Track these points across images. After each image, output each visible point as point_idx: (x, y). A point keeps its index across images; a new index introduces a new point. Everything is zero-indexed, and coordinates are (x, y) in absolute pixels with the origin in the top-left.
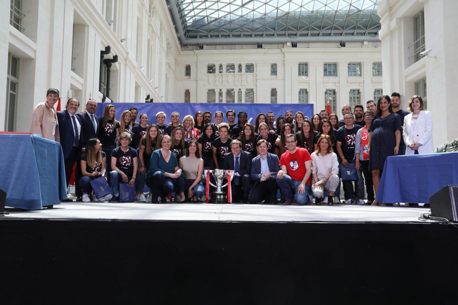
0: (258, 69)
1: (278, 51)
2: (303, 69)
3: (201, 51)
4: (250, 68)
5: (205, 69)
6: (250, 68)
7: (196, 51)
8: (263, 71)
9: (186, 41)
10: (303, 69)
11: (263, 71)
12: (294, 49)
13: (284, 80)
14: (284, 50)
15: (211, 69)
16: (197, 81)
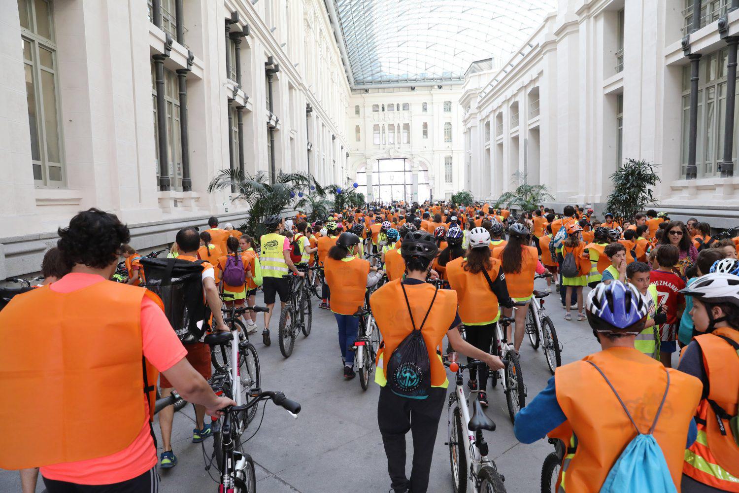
0: (412, 108)
1: (427, 92)
2: (448, 107)
3: (367, 94)
4: (406, 107)
5: (371, 109)
6: (406, 107)
7: (363, 95)
8: (417, 109)
9: (354, 87)
10: (448, 107)
11: (417, 109)
12: (441, 91)
13: (433, 115)
14: (432, 92)
15: (376, 108)
16: (365, 118)
